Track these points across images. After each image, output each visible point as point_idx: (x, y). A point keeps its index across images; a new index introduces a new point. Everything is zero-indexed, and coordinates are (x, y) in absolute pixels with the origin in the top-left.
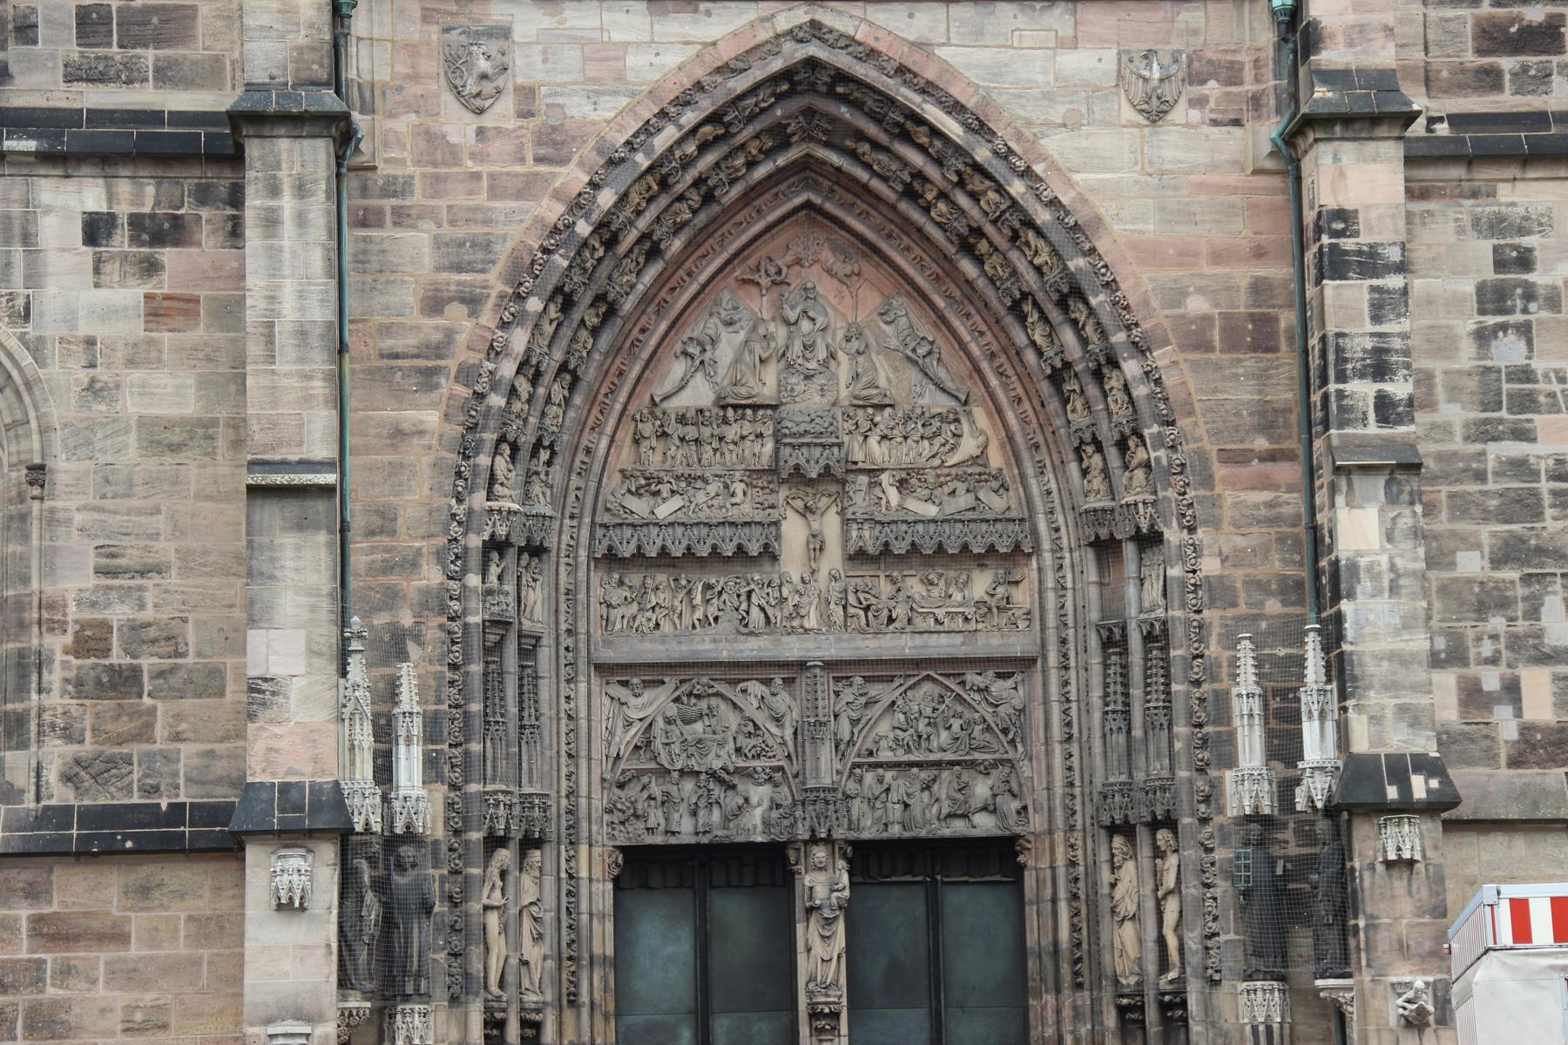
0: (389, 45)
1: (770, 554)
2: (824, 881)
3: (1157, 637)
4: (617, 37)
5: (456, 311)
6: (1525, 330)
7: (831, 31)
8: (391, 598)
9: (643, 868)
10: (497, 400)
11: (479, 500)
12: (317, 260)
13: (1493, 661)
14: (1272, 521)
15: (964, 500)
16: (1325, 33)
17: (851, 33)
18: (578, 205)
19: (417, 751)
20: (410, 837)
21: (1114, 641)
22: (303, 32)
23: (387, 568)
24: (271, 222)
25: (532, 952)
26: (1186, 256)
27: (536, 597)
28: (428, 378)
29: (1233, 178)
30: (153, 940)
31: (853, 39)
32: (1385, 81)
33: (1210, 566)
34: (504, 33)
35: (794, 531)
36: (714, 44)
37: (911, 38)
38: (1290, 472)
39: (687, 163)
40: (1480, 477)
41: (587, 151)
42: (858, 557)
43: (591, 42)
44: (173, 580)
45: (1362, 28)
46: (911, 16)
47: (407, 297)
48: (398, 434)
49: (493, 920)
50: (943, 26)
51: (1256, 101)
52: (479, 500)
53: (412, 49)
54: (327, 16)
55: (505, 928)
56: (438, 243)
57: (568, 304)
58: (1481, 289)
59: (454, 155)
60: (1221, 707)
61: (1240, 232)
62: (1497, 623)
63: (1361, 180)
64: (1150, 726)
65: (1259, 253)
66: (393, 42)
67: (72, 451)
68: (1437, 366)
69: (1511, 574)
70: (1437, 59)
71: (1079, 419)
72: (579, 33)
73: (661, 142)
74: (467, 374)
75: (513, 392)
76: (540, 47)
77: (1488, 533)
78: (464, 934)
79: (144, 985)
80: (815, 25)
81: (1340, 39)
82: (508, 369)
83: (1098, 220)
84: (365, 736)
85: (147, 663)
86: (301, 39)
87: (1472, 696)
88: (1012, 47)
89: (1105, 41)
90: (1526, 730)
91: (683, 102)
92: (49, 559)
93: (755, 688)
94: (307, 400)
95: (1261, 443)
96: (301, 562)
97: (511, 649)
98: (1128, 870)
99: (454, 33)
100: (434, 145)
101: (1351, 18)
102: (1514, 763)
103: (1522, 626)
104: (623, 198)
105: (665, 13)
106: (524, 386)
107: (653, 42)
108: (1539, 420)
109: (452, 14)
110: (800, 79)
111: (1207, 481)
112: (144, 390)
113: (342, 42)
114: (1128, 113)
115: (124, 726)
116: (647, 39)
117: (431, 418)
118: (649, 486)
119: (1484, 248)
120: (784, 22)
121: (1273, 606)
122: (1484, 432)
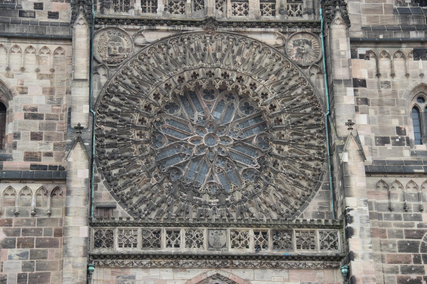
0: (102, 281)
4: (164, 278)
7: (222, 276)
16: (357, 279)
17: (228, 277)
22: (79, 279)
31: (228, 278)
34: (133, 277)
36: (190, 280)
37: (244, 278)
43: (157, 279)
45: (367, 278)
46: (244, 272)
50: (252, 276)
54: (85, 274)
66: (103, 280)
72: (154, 277)
76: (143, 281)
80: (218, 275)
81: (361, 281)
86: (78, 280)
88: (271, 281)
89: (297, 280)
99: (120, 278)
101: (364, 276)
105: (177, 272)
107: (174, 279)
109: (119, 273)
113: (89, 281)
116: (172, 278)
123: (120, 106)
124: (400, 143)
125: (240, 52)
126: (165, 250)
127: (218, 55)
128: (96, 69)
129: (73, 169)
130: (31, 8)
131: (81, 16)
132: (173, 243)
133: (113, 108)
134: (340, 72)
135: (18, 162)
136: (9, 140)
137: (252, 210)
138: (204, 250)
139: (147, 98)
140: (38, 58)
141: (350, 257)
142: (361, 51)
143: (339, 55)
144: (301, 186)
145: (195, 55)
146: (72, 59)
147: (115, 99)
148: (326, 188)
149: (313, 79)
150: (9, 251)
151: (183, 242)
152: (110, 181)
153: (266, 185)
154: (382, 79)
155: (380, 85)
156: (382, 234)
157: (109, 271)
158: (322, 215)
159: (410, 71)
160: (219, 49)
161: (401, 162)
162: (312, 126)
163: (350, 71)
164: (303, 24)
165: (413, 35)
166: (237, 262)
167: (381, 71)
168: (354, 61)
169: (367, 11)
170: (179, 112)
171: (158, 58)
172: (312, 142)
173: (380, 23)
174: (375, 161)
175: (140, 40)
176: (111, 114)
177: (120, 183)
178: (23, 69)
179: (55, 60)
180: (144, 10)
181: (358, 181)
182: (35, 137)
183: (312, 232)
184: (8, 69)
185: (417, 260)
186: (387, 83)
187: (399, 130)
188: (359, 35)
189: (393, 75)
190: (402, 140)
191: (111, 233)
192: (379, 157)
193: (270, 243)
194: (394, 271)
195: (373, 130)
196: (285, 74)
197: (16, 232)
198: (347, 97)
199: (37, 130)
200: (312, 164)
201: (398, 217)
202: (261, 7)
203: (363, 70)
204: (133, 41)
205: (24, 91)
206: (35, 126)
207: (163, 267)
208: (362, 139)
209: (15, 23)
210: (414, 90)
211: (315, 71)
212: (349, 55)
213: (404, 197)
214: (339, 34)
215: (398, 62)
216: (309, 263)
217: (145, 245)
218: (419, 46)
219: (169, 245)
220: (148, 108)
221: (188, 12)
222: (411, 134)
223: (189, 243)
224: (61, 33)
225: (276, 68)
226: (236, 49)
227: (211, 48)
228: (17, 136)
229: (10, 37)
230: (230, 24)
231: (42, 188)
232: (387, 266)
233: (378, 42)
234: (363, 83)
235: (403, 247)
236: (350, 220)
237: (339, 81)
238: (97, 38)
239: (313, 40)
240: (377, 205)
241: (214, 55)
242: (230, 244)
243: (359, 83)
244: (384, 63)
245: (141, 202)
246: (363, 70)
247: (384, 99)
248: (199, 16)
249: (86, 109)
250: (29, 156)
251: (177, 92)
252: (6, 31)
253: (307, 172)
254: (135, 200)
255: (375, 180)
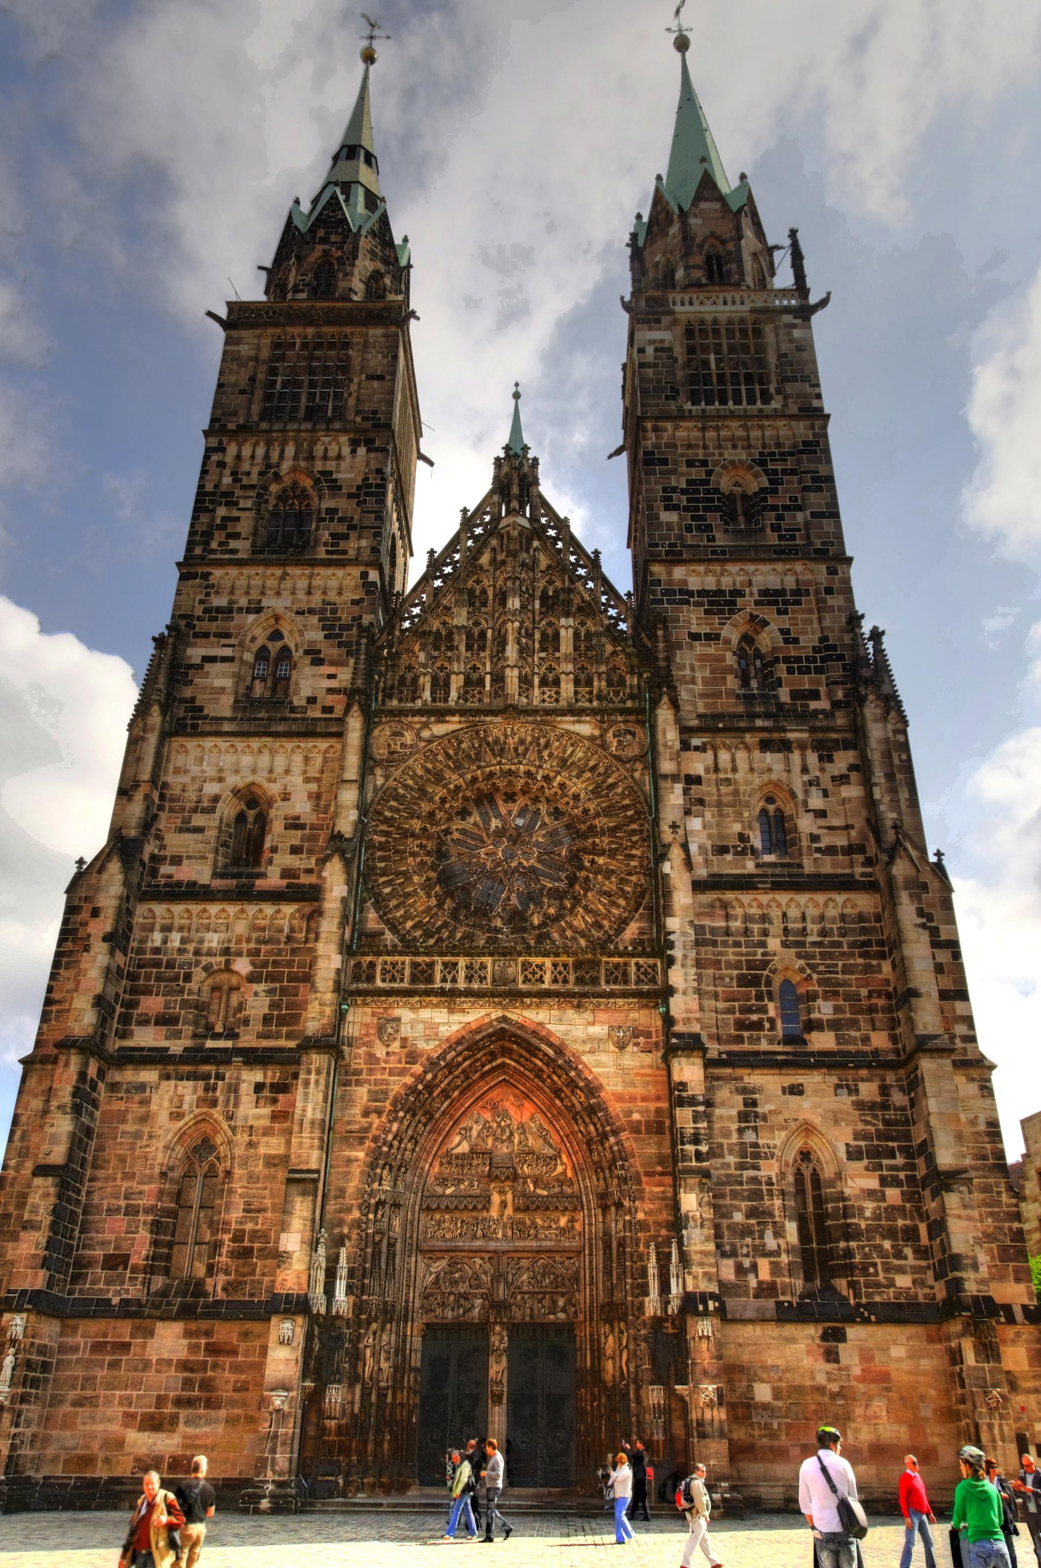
1: (486, 1208)
2: (499, 1339)
3: (622, 1244)
5: (374, 1117)
6: (755, 1129)
8: (341, 1223)
9: (431, 1330)
10: (385, 1149)
11: (376, 1186)
12: (321, 1096)
13: (747, 1255)
14: (664, 1199)
15: (557, 1189)
18: (419, 1079)
19: (344, 1283)
20: (338, 1317)
21: (607, 1246)
23: (341, 1211)
24: (307, 1083)
25: (384, 1365)
26: (633, 1099)
27: (397, 1223)
28: (361, 1140)
29: (648, 1071)
30: (247, 1354)
32: (696, 1037)
33: (641, 1216)
34: (398, 1020)
35: (496, 1199)
38: (668, 1180)
39: (459, 1064)
40: (741, 1183)
41: (423, 1059)
42: (517, 1209)
44: (269, 1214)
47: (357, 1111)
48: (349, 1161)
49: (368, 1352)
51: (656, 1044)
52: (376, 1186)
53: (367, 1025)
55: (373, 1355)
56: (369, 1092)
57: (413, 1116)
58: (739, 1113)
59: (377, 1061)
60: (644, 1272)
61: (652, 1090)
62: (748, 1240)
63: (689, 1071)
64: (619, 1278)
65: (658, 1098)
67: (240, 1166)
68: (725, 1141)
69: (753, 1221)
70: (722, 1031)
71: (596, 1158)
73: (449, 1057)
74: (375, 1139)
75: (391, 1146)
77: (744, 1205)
78: (356, 1357)
79: (242, 1372)
82: (390, 1137)
83: (600, 1087)
84: (321, 1276)
85: (256, 1245)
87: (740, 1270)
90: (760, 1283)
91: (459, 1042)
92: (228, 1205)
93: (478, 1261)
94: (312, 1147)
95: (659, 1169)
96: (302, 1209)
97: (385, 1243)
98: (611, 1339)
100: (372, 1058)
102: (756, 1296)
103: (757, 1242)
104: (435, 1077)
106: (396, 1143)
108: (761, 1162)
110: (500, 1034)
111: (640, 1183)
112: (267, 1145)
114: (612, 1048)
115: (246, 1270)
117: (361, 1155)
118: (443, 1182)
119: (739, 1099)
120: (493, 1016)
121: (664, 1232)
122: (741, 1167)
123: (398, 810)
124: (743, 853)
125: (547, 745)
126: (438, 985)
127: (521, 749)
128: (372, 769)
129: (328, 885)
130: (303, 703)
131: (355, 708)
132: (449, 977)
133: (388, 814)
134: (667, 766)
135: (273, 879)
136: (267, 855)
137: (556, 936)
138: (487, 985)
139: (431, 800)
140: (307, 760)
141: (669, 991)
142: (696, 742)
143: (666, 745)
144: (618, 906)
145: (492, 750)
146: (342, 757)
147: (393, 803)
148: (649, 908)
149: (637, 775)
150: (255, 987)
151: (462, 975)
152: (380, 902)
153: (573, 906)
154: (722, 776)
155: (719, 783)
156: (717, 965)
157: (369, 1010)
158: (641, 942)
159: (756, 766)
160: (522, 742)
161: (743, 876)
162: (633, 832)
163: (679, 764)
164: (624, 712)
165: (759, 723)
166: (528, 1001)
167: (721, 766)
168: (688, 754)
169: (703, 696)
170: (472, 820)
171: (447, 754)
172: (634, 852)
173: (719, 710)
174: (711, 875)
175: (426, 734)
176: (388, 821)
177: (394, 902)
178: (287, 772)
179: (325, 760)
180: (434, 700)
181: (682, 897)
182: (295, 850)
183: (626, 964)
184: (271, 771)
185: (759, 997)
186: (727, 780)
187: (742, 838)
188: (695, 723)
189: (734, 770)
190: (745, 848)
191: (372, 965)
192: (715, 870)
193: (572, 978)
194: (730, 1011)
195: (710, 837)
196: (601, 770)
197: (265, 964)
198: (674, 797)
199: (298, 842)
200: (633, 878)
201: (737, 944)
202: (576, 693)
203: (698, 764)
204: (418, 735)
205: (286, 797)
206: (296, 837)
207: (436, 1006)
208: (693, 848)
209: (284, 719)
210: (761, 788)
211: (639, 766)
212: (677, 745)
213: (747, 918)
214: (666, 721)
215: (741, 755)
216: (620, 1001)
217: (414, 979)
218: (765, 735)
219: (444, 980)
220: (431, 814)
221: (486, 700)
222: (757, 842)
223: (469, 978)
224: (334, 729)
225: (592, 763)
226: (542, 741)
227: (512, 742)
228: (274, 850)
229: (276, 735)
230: (535, 712)
231: (298, 911)
232: (721, 1005)
233: (719, 730)
234: (696, 780)
235: (742, 981)
236: (671, 945)
237: (665, 777)
238: (376, 733)
239: (638, 730)
240: (713, 930)
241: (516, 749)
242: (521, 979)
243: (693, 780)
244: (724, 756)
245: (414, 927)
246: (698, 764)
247: (724, 799)
248: (499, 703)
249: (353, 815)
250: (287, 873)
251: (468, 793)
252: (273, 729)
253: (627, 889)
254: (409, 924)
255: (707, 897)
